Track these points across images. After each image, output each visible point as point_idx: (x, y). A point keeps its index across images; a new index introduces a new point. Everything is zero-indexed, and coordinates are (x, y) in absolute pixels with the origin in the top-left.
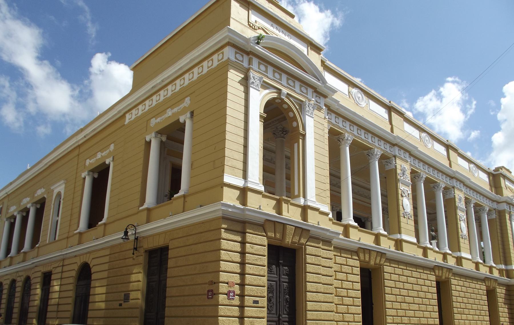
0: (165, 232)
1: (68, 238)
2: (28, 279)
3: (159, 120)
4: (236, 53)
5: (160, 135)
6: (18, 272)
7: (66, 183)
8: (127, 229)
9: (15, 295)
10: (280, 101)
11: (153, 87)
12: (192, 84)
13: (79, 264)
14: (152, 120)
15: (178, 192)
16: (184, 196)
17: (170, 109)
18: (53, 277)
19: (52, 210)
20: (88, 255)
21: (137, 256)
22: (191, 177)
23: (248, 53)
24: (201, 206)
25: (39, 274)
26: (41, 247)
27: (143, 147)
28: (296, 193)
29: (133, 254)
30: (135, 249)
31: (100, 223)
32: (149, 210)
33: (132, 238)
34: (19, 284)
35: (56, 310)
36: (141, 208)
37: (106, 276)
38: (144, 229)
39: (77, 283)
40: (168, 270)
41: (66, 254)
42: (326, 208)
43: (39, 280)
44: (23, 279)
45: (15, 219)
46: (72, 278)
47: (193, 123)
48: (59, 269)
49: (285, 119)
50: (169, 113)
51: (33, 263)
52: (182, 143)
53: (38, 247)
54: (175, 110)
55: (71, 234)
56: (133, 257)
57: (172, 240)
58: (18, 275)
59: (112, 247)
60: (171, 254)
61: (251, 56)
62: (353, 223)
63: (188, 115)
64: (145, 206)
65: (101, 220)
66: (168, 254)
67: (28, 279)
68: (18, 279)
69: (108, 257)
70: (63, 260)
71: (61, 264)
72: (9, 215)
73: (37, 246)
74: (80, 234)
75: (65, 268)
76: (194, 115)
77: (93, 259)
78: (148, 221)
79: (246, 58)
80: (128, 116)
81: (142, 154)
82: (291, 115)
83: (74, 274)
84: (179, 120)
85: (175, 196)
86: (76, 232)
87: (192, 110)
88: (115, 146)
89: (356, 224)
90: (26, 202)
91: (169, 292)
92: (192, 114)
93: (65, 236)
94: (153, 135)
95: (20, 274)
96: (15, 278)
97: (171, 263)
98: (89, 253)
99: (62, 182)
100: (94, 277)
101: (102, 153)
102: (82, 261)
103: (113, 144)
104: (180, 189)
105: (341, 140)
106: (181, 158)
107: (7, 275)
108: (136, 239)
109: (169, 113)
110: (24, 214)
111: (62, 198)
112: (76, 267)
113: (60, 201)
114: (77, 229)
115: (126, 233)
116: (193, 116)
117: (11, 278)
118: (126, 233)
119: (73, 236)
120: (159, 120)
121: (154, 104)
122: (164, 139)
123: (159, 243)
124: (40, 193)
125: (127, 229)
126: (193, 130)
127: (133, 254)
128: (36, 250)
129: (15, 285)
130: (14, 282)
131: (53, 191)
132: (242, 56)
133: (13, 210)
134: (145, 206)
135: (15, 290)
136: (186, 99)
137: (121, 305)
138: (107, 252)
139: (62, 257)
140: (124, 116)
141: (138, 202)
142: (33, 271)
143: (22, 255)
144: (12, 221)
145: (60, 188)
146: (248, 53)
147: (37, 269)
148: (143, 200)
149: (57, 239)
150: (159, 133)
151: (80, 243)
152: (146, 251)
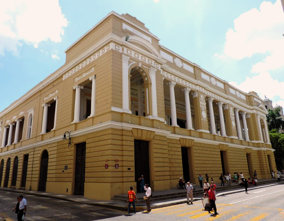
0: (84, 135)
1: (36, 137)
2: (16, 158)
3: (79, 79)
4: (116, 46)
5: (80, 86)
6: (11, 154)
7: (34, 109)
8: (65, 134)
9: (10, 166)
10: (138, 68)
11: (75, 63)
12: (95, 61)
13: (42, 150)
14: (76, 78)
15: (89, 115)
17: (84, 73)
18: (29, 157)
19: (28, 123)
20: (47, 146)
21: (71, 147)
23: (122, 45)
24: (101, 123)
25: (22, 155)
26: (23, 141)
27: (72, 92)
28: (148, 113)
29: (69, 146)
30: (70, 143)
31: (52, 130)
32: (76, 124)
33: (67, 138)
34: (12, 160)
35: (31, 174)
36: (72, 123)
37: (56, 157)
38: (74, 134)
39: (42, 160)
41: (35, 145)
43: (22, 158)
44: (14, 157)
45: (9, 127)
46: (38, 158)
47: (96, 81)
48: (32, 153)
49: (141, 76)
50: (84, 75)
51: (19, 150)
53: (21, 142)
54: (87, 74)
55: (37, 135)
57: (87, 139)
58: (11, 156)
59: (58, 142)
60: (87, 146)
61: (123, 47)
62: (177, 125)
63: (94, 77)
64: (74, 122)
65: (52, 129)
66: (85, 146)
67: (16, 158)
68: (12, 158)
69: (56, 147)
70: (34, 148)
71: (33, 150)
72: (6, 125)
73: (21, 141)
74: (42, 135)
75: (35, 153)
77: (49, 148)
78: (76, 130)
79: (121, 48)
80: (64, 76)
81: (71, 96)
82: (144, 74)
83: (40, 155)
84: (89, 79)
85: (88, 117)
86: (40, 134)
88: (58, 91)
89: (179, 126)
90: (15, 118)
91: (87, 165)
92: (95, 75)
93: (35, 136)
94: (77, 86)
95: (13, 155)
96: (10, 157)
97: (87, 151)
98: (47, 145)
99: (33, 109)
100: (49, 157)
101: (52, 94)
102: (43, 149)
103: (57, 90)
105: (170, 85)
106: (91, 96)
107: (6, 155)
108: (70, 138)
109: (84, 75)
110: (14, 124)
111: (33, 117)
112: (41, 152)
113: (32, 119)
114: (40, 133)
115: (65, 136)
116: (96, 77)
117: (8, 157)
118: (65, 136)
119: (38, 136)
120: (79, 79)
121: (76, 71)
122: (82, 88)
123: (81, 140)
124: (21, 114)
125: (65, 134)
126: (96, 85)
127: (69, 146)
128: (21, 143)
129: (10, 161)
130: (9, 159)
131: (28, 113)
132: (119, 47)
133: (8, 122)
134: (74, 122)
135: (10, 163)
136: (92, 68)
137: (63, 171)
138: (56, 145)
139: (33, 147)
140: (62, 76)
141: (70, 120)
142: (19, 154)
143: (13, 146)
144: (8, 128)
145: (31, 112)
146: (122, 45)
147: (21, 153)
148: (73, 119)
149: (31, 137)
150: (80, 85)
151: (42, 140)
152: (75, 144)
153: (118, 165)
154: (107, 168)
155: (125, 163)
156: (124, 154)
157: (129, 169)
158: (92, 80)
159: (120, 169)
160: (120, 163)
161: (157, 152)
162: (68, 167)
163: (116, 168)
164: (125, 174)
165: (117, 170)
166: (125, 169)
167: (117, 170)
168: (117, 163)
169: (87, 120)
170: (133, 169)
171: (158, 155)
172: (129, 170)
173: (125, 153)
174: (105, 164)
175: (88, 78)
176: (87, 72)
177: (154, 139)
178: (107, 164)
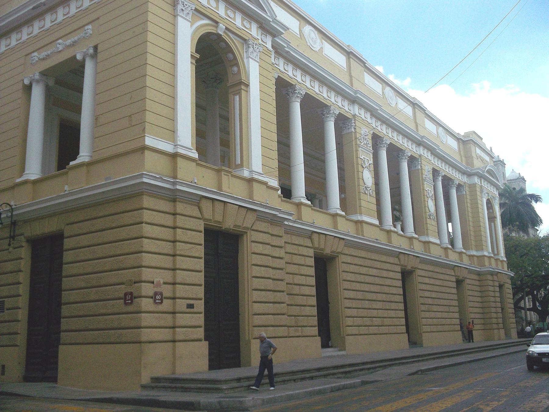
15: (75, 158)
16: (88, 165)
21: (15, 248)
22: (95, 138)
40: (64, 266)
42: (274, 183)
52: (80, 90)
56: (8, 249)
76: (99, 51)
85: (72, 163)
87: (95, 44)
92: (96, 48)
97: (67, 256)
104: (79, 154)
109: (60, 45)
126: (96, 73)
153: (161, 294)
154: (131, 303)
155: (180, 291)
156: (178, 267)
157: (191, 306)
158: (84, 60)
159: (167, 305)
160: (167, 291)
161: (259, 263)
162: (7, 305)
163: (155, 301)
164: (182, 320)
165: (161, 308)
166: (181, 305)
167: (161, 308)
168: (158, 290)
169: (67, 173)
170: (200, 306)
171: (262, 272)
172: (189, 310)
173: (181, 262)
174: (124, 292)
175: (74, 54)
176: (69, 36)
177: (253, 230)
178: (129, 291)
